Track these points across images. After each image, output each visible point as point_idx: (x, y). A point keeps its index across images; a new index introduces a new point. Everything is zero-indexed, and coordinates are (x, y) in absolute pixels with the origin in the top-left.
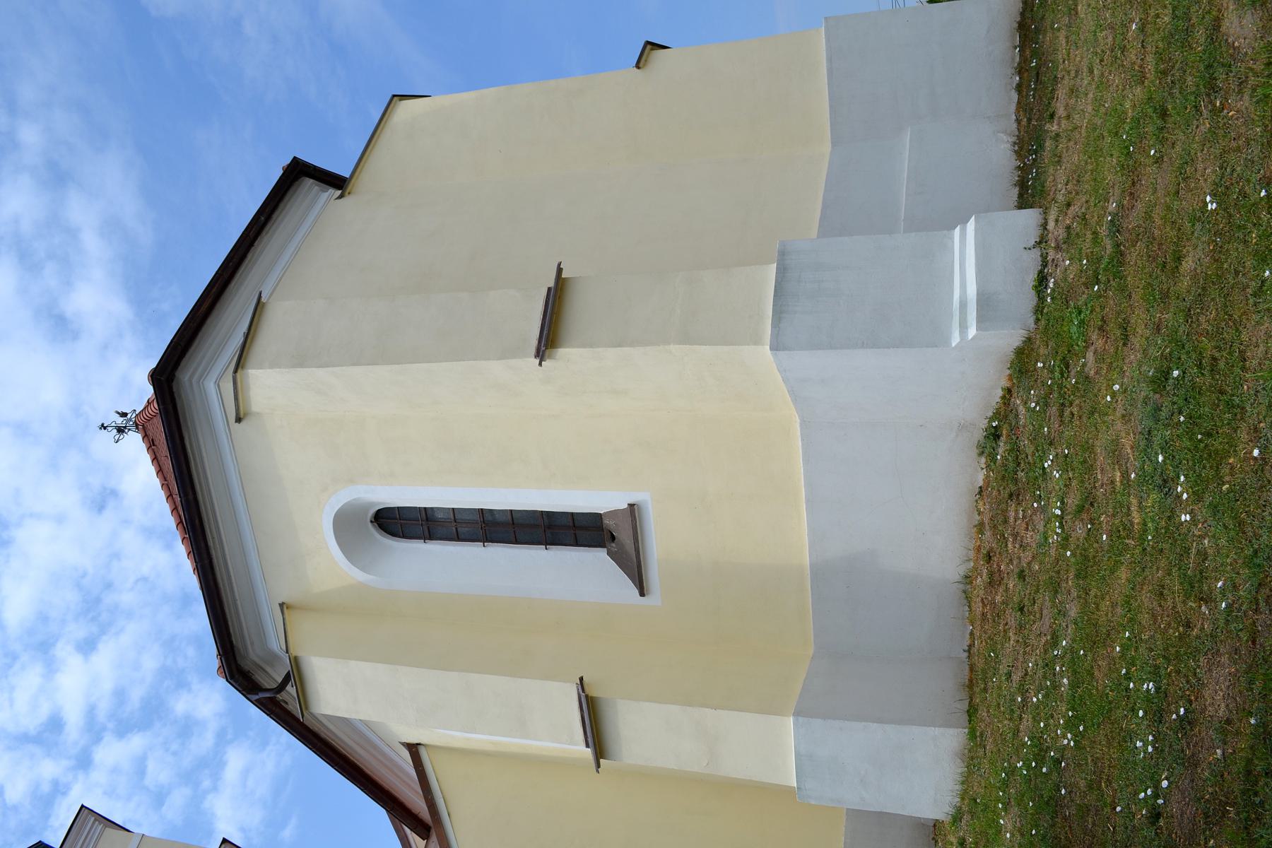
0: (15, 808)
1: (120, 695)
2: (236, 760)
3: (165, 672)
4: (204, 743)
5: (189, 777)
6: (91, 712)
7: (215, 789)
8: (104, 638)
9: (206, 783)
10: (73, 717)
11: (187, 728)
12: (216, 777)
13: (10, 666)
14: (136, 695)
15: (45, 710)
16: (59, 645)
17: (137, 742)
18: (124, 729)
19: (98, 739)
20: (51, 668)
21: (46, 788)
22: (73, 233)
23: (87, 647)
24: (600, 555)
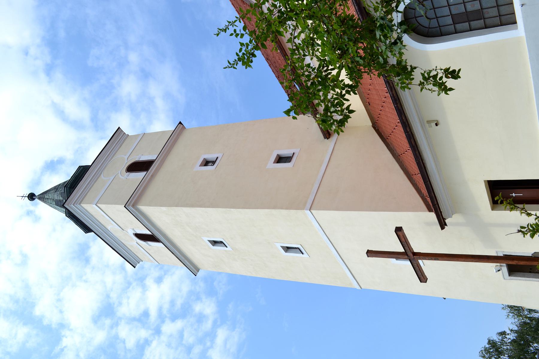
0: (130, 350)
1: (172, 303)
2: (222, 334)
3: (191, 293)
4: (208, 325)
5: (201, 341)
6: (160, 309)
7: (211, 347)
8: (166, 276)
9: (208, 344)
10: (153, 313)
11: (201, 318)
12: (213, 340)
13: (128, 287)
14: (179, 302)
15: (142, 308)
16: (147, 279)
17: (179, 324)
18: (174, 318)
19: (163, 322)
20: (144, 288)
21: (142, 342)
22: (151, 100)
23: (159, 280)
24: (415, 251)
